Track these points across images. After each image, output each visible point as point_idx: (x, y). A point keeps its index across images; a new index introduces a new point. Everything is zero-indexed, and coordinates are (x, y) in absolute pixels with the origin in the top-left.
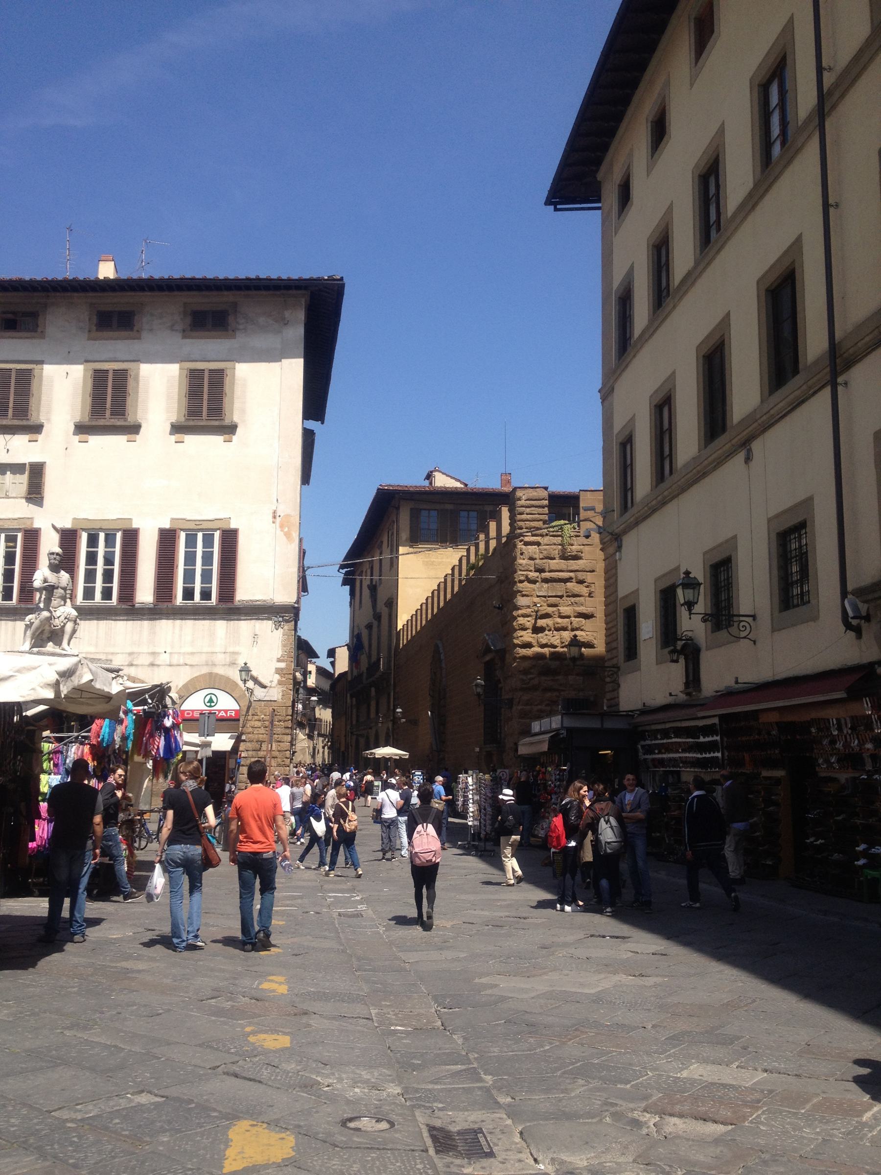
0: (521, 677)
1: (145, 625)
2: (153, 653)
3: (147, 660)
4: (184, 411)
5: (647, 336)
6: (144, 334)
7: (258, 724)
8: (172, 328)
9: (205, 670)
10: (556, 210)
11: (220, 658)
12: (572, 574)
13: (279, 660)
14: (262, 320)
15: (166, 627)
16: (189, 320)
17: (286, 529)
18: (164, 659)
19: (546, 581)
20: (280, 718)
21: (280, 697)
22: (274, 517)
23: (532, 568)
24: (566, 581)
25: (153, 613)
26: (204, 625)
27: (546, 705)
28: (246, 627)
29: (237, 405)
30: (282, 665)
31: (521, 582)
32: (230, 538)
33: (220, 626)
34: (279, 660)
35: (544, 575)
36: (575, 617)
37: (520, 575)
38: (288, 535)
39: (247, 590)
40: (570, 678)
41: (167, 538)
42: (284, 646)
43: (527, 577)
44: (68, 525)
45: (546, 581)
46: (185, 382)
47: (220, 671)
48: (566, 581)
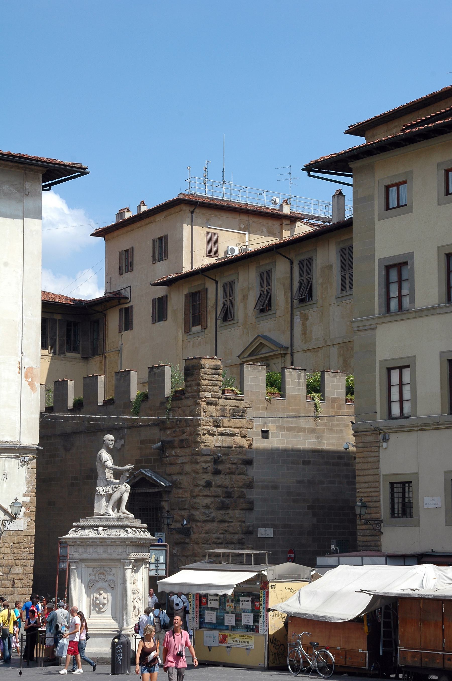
0: (203, 510)
7: (8, 551)
10: (309, 175)
12: (238, 430)
13: (24, 495)
17: (30, 380)
19: (222, 434)
20: (26, 545)
21: (26, 527)
22: (19, 368)
23: (212, 424)
24: (233, 435)
27: (220, 534)
30: (28, 499)
31: (204, 434)
34: (24, 495)
35: (220, 430)
36: (242, 464)
37: (202, 429)
38: (31, 385)
40: (237, 512)
42: (28, 482)
43: (208, 431)
45: (222, 434)
48: (233, 435)
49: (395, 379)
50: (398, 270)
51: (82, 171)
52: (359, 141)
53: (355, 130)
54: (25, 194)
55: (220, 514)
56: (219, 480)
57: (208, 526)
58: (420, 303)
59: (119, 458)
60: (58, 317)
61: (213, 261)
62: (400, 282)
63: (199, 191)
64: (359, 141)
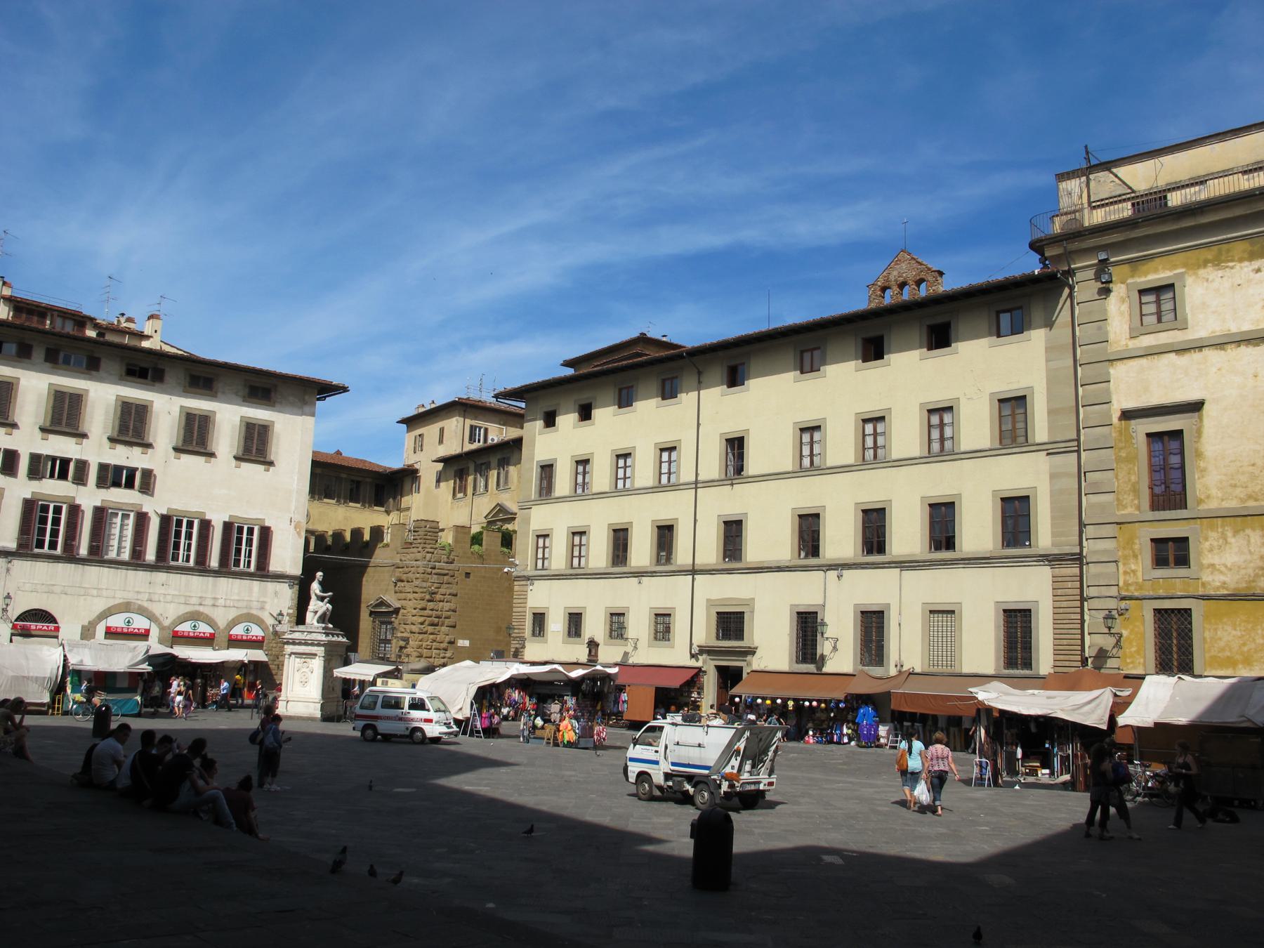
1: (210, 580)
2: (215, 599)
3: (210, 602)
4: (241, 449)
5: (545, 483)
6: (219, 395)
8: (236, 394)
9: (245, 611)
11: (255, 604)
14: (291, 398)
15: (224, 582)
16: (247, 390)
18: (221, 602)
25: (217, 573)
26: (246, 583)
28: (271, 586)
29: (273, 449)
32: (266, 533)
33: (256, 585)
38: (299, 533)
39: (275, 566)
41: (228, 526)
44: (165, 512)
46: (244, 429)
47: (254, 612)
49: (541, 544)
50: (547, 470)
51: (344, 389)
52: (570, 372)
53: (568, 364)
54: (304, 403)
55: (430, 629)
56: (431, 605)
57: (421, 636)
58: (596, 489)
59: (325, 588)
60: (368, 480)
61: (475, 446)
62: (585, 473)
63: (475, 396)
64: (570, 372)
